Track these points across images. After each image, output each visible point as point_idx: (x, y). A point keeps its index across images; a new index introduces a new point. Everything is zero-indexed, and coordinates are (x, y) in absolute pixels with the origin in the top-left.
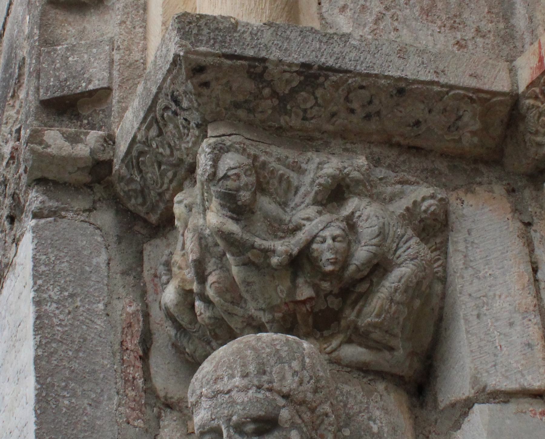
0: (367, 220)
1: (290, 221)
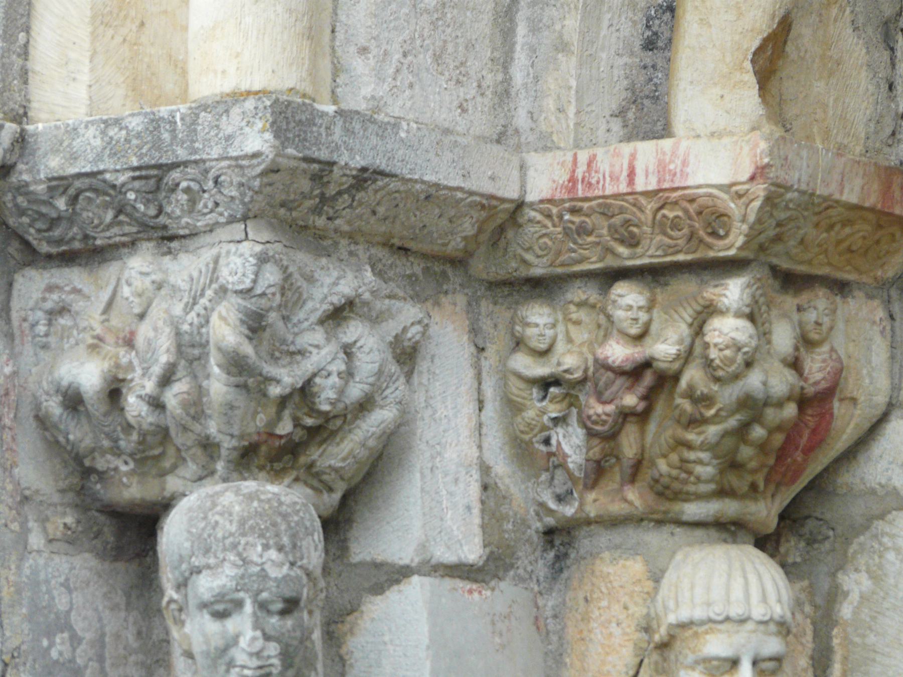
0: (368, 353)
1: (293, 343)
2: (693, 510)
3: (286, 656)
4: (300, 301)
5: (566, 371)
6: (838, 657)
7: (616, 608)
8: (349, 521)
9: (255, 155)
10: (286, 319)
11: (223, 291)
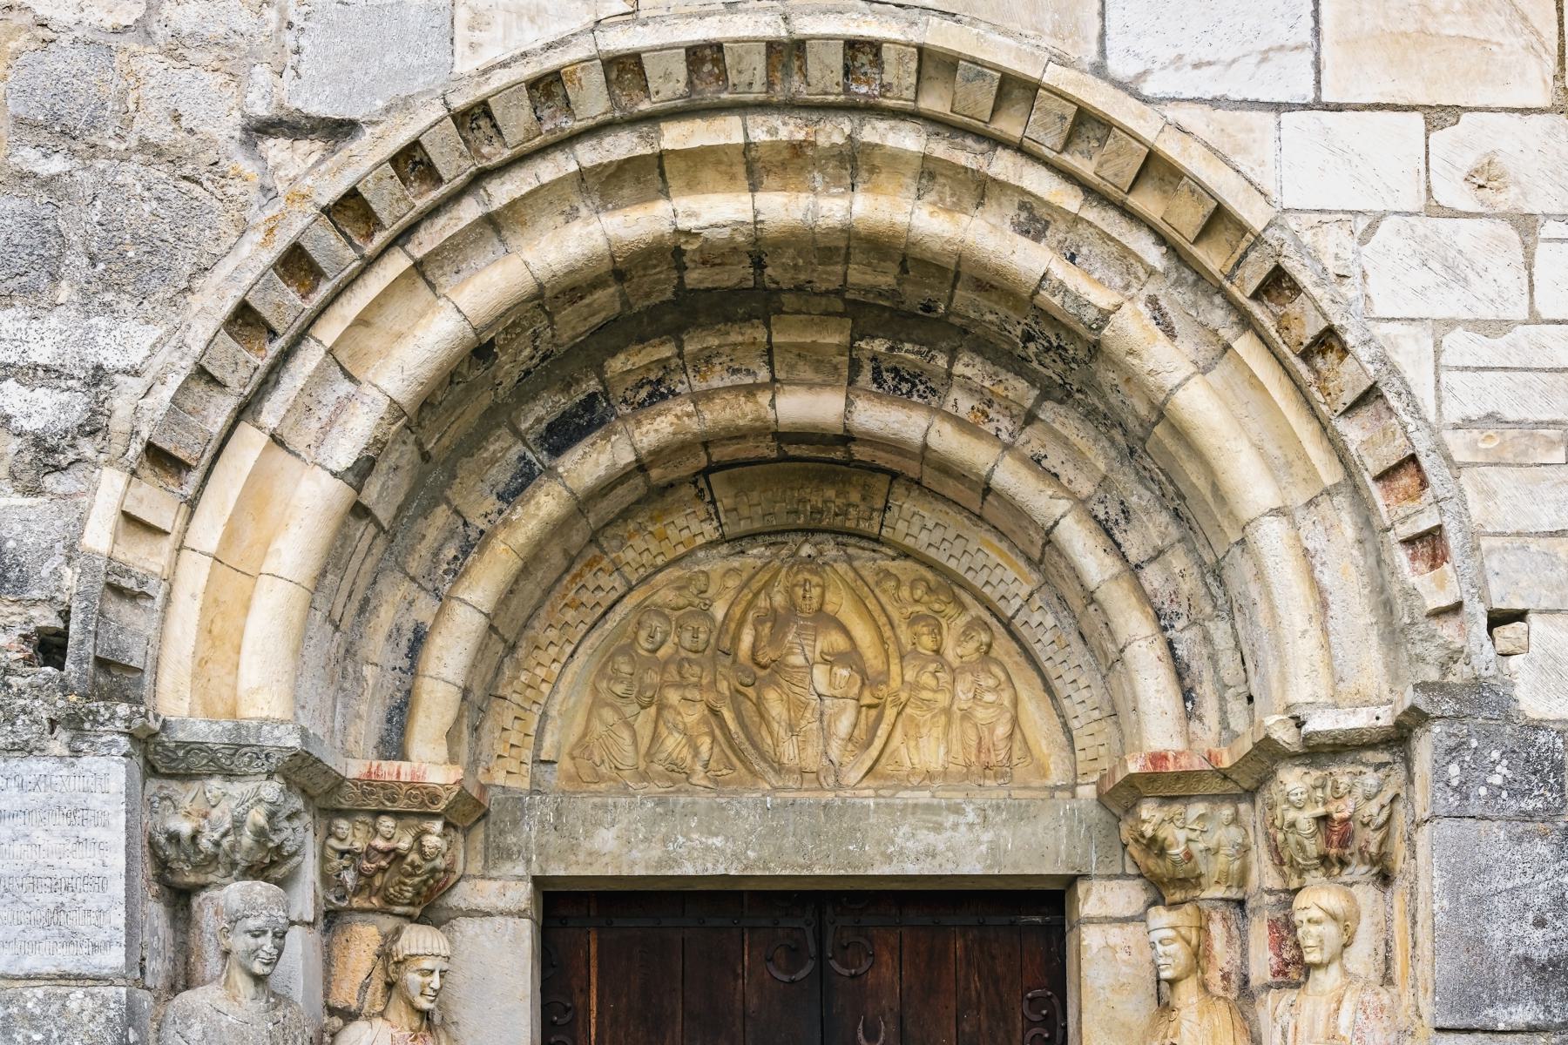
11: (260, 800)
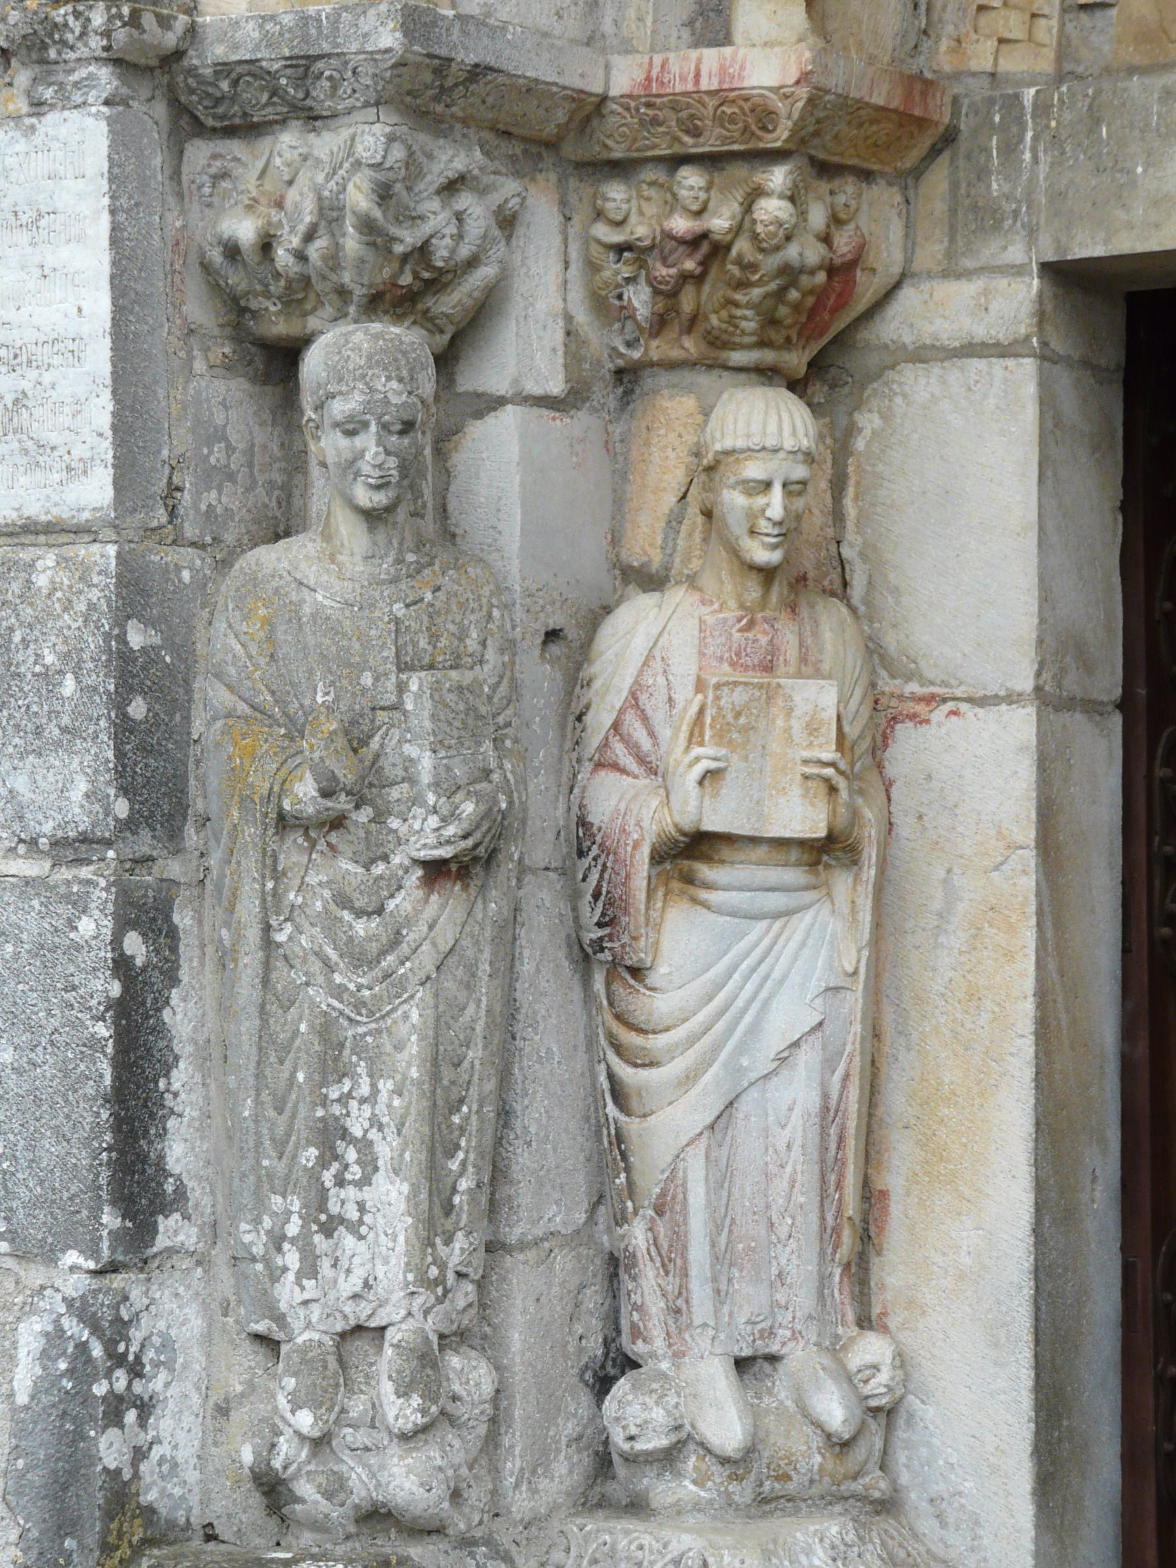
2: (738, 357)
3: (403, 468)
4: (420, 174)
5: (638, 239)
6: (852, 482)
7: (672, 436)
8: (456, 358)
9: (387, 51)
10: (409, 189)
11: (358, 164)
